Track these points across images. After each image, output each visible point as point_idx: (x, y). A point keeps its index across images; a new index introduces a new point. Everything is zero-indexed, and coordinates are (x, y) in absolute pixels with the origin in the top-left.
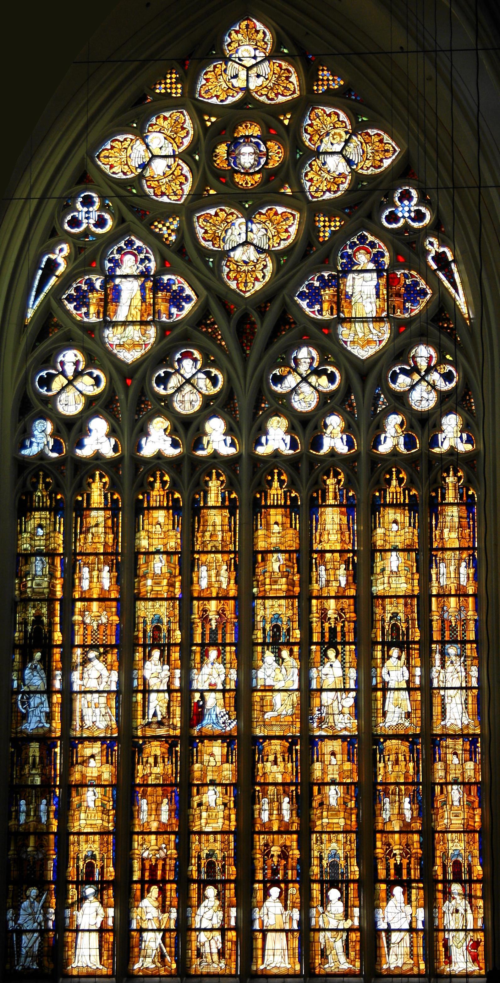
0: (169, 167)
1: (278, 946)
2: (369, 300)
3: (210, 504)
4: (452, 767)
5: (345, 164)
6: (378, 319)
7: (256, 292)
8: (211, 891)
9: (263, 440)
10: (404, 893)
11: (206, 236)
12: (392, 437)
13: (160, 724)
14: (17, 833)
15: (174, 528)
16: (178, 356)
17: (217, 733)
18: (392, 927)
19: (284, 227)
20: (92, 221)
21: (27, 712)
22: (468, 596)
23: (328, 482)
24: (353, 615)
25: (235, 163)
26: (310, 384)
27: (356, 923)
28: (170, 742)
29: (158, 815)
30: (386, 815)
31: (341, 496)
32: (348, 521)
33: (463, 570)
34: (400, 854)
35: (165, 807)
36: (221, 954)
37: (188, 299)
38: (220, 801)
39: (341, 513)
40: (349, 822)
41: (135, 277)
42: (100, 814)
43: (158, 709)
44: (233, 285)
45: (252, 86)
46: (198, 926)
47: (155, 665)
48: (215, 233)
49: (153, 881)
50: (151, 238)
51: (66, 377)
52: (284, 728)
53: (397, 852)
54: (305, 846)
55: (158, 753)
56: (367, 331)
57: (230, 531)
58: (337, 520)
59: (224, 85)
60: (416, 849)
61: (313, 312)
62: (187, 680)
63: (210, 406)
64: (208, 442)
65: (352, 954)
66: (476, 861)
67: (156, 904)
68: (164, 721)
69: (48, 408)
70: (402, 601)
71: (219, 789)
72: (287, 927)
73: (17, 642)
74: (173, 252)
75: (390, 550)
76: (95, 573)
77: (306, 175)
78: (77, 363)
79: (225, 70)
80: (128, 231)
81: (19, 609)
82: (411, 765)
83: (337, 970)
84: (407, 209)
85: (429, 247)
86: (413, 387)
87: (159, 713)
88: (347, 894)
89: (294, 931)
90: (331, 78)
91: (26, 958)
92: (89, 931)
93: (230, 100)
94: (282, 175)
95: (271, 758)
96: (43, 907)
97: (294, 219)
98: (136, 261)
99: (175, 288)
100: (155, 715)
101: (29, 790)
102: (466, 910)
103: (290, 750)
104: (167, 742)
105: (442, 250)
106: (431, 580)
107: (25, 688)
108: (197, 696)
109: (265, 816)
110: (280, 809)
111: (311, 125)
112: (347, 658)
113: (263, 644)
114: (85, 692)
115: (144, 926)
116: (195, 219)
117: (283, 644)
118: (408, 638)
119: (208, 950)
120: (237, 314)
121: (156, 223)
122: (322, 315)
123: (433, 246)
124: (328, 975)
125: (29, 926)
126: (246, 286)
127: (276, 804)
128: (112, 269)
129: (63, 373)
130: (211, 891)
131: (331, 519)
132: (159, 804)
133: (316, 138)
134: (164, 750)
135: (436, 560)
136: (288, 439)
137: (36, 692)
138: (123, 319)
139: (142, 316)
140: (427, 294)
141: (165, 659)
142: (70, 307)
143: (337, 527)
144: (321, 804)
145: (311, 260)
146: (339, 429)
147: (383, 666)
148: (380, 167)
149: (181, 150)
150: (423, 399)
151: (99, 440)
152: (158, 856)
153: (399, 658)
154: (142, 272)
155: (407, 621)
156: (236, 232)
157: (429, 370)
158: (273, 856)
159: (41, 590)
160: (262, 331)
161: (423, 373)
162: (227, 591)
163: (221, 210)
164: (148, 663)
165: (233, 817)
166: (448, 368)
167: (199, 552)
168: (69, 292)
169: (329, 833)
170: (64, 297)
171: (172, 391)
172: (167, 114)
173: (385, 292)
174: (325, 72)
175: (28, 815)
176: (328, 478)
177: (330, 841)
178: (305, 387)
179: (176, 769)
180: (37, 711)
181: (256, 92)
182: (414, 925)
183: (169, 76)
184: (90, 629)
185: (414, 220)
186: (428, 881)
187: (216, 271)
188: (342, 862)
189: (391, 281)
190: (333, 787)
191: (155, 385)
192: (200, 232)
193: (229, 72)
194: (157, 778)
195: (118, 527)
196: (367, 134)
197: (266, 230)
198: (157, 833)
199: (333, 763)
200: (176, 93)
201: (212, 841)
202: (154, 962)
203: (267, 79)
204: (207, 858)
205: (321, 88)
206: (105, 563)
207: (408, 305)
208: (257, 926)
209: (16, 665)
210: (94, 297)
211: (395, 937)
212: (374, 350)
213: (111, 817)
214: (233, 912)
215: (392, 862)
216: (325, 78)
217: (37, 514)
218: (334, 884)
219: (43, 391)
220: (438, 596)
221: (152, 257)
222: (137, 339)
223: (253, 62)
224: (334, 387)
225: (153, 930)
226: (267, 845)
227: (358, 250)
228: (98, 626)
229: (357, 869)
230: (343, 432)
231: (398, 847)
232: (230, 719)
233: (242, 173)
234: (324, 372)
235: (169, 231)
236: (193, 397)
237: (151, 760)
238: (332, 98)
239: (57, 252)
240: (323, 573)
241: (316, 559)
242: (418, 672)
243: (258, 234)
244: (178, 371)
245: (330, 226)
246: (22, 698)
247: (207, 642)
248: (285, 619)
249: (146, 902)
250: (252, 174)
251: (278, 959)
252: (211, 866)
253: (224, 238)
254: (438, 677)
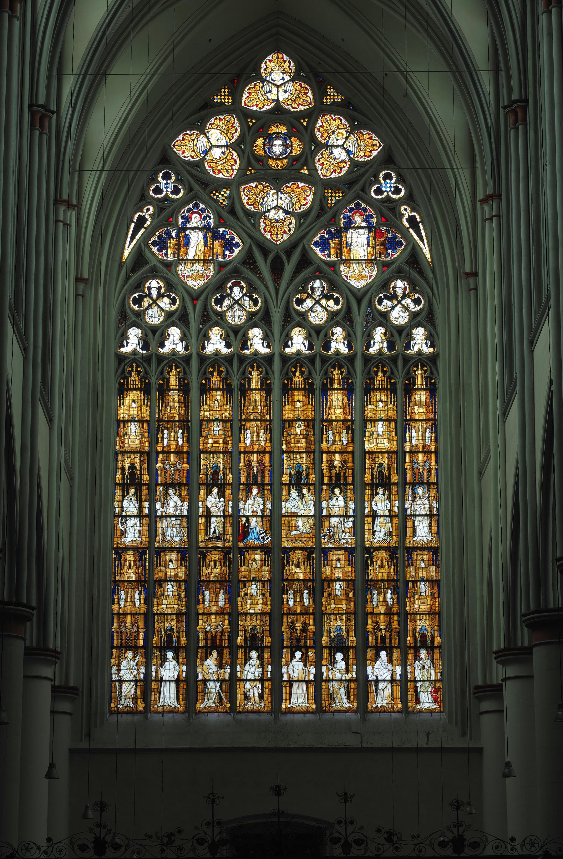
0: (223, 153)
1: (300, 691)
2: (363, 248)
3: (252, 387)
4: (421, 569)
5: (345, 154)
6: (368, 262)
7: (284, 241)
8: (254, 654)
9: (290, 343)
10: (387, 656)
11: (249, 201)
12: (379, 342)
13: (218, 539)
14: (119, 614)
15: (227, 404)
16: (230, 284)
17: (258, 545)
18: (379, 679)
19: (304, 197)
20: (169, 190)
21: (126, 530)
22: (431, 452)
23: (334, 373)
24: (352, 464)
25: (269, 151)
26: (321, 305)
27: (355, 676)
28: (226, 552)
29: (217, 602)
30: (374, 603)
31: (344, 382)
32: (348, 400)
33: (427, 434)
34: (385, 629)
35: (221, 596)
36: (261, 697)
37: (237, 245)
38: (260, 592)
39: (344, 394)
40: (349, 607)
41: (200, 229)
42: (176, 601)
43: (217, 528)
44: (268, 236)
45: (281, 99)
46: (245, 678)
47: (215, 498)
48: (255, 199)
49: (214, 647)
50: (211, 202)
51: (151, 298)
52: (304, 542)
53: (382, 627)
54: (319, 624)
55: (217, 559)
56: (361, 269)
57: (267, 406)
58: (340, 399)
59: (262, 98)
60: (395, 625)
61: (324, 256)
62: (236, 508)
63: (253, 320)
64: (251, 344)
65: (352, 697)
66: (436, 634)
67: (215, 663)
68: (221, 536)
69: (138, 320)
70: (385, 455)
71: (259, 584)
72: (307, 678)
73: (118, 482)
74: (227, 212)
75: (377, 420)
76: (172, 434)
77: (319, 161)
78: (159, 289)
79: (262, 87)
80: (196, 197)
81: (120, 457)
82: (392, 568)
83: (341, 708)
84: (388, 185)
85: (404, 212)
86: (393, 308)
87: (217, 531)
88: (348, 656)
89: (312, 681)
90: (336, 94)
91: (126, 699)
92: (170, 681)
93: (266, 108)
94: (302, 160)
95: (295, 562)
96: (137, 664)
97: (310, 191)
98: (201, 218)
99: (227, 237)
100: (215, 532)
101: (126, 584)
102: (430, 667)
103: (308, 558)
104: (223, 551)
105: (413, 214)
106: (405, 441)
107: (124, 514)
108: (244, 519)
109: (291, 603)
110: (301, 598)
111: (322, 126)
112: (349, 494)
113: (290, 485)
114: (166, 517)
115: (207, 678)
116: (242, 190)
117: (303, 484)
118: (390, 480)
119: (252, 694)
120: (271, 257)
121: (214, 192)
122: (330, 257)
123: (406, 212)
124: (336, 712)
125: (128, 677)
126: (277, 237)
127: (299, 594)
128: (184, 224)
129: (150, 295)
130: (254, 654)
131: (337, 399)
132: (217, 595)
133: (325, 135)
134: (221, 557)
135: (409, 427)
136: (306, 343)
137: (131, 516)
138: (192, 258)
139: (205, 256)
140: (403, 244)
141: (221, 494)
142: (155, 249)
143: (340, 404)
144: (330, 594)
145: (323, 219)
146: (342, 336)
147: (372, 500)
148: (370, 156)
149: (231, 142)
150: (399, 317)
151: (174, 342)
152: (217, 629)
153: (384, 494)
154: (205, 226)
155: (389, 469)
156: (270, 199)
157: (403, 297)
158: (297, 630)
159: (135, 446)
160: (289, 269)
161: (400, 299)
162: (265, 447)
163: (260, 184)
164: (209, 497)
165: (269, 603)
166: (417, 296)
167: (245, 420)
168: (153, 239)
169: (335, 614)
170: (150, 242)
171: (226, 309)
172: (222, 117)
173: (374, 242)
174: (332, 90)
175: (126, 601)
176: (335, 370)
177: (336, 620)
178: (318, 307)
179: (229, 570)
180: (132, 529)
181: (284, 103)
182: (394, 677)
183: (223, 90)
184: (169, 473)
185: (393, 193)
186: (404, 648)
187: (256, 226)
188: (345, 634)
189: (378, 234)
190: (338, 583)
191: (213, 304)
192: (245, 199)
193: (265, 89)
194: (216, 576)
195: (188, 402)
196: (361, 133)
197: (291, 198)
198: (216, 614)
199: (337, 567)
200: (228, 102)
201: (254, 619)
202: (214, 703)
203: (291, 94)
204: (251, 631)
205: (328, 101)
206: (180, 428)
207: (390, 252)
208: (285, 678)
209: (118, 498)
210: (171, 243)
211: (381, 685)
212: (366, 282)
213: (184, 603)
214: (269, 668)
215: (379, 634)
216: (332, 94)
217: (132, 393)
218: (339, 650)
219: (136, 308)
220: (411, 452)
221: (212, 216)
222: (202, 272)
223: (282, 82)
224: (338, 307)
225: (214, 681)
226: (292, 622)
227: (355, 213)
228: (174, 470)
229: (354, 639)
230: (344, 339)
231: (384, 624)
232: (267, 535)
233: (274, 159)
234: (331, 297)
235: (224, 198)
236: (240, 313)
237: (212, 564)
238: (334, 109)
239: (145, 211)
240: (331, 436)
241: (326, 426)
242: (397, 504)
243: (285, 201)
244: (229, 295)
245: (335, 197)
246: (122, 520)
247: (251, 482)
248: (304, 467)
249: (208, 662)
250: (281, 159)
251: (300, 700)
252: (254, 636)
253: (262, 203)
254: (411, 508)
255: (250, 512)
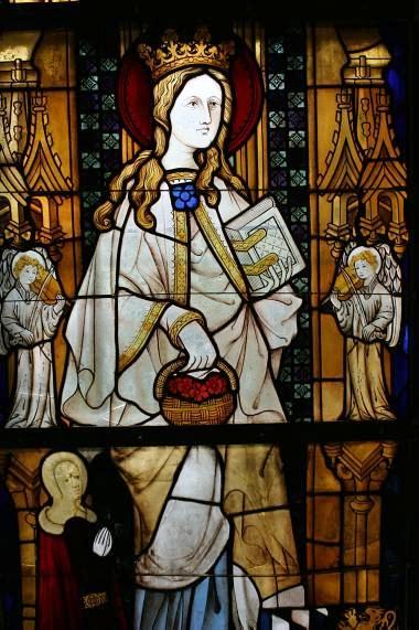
108: (64, 474)
255: (140, 384)
